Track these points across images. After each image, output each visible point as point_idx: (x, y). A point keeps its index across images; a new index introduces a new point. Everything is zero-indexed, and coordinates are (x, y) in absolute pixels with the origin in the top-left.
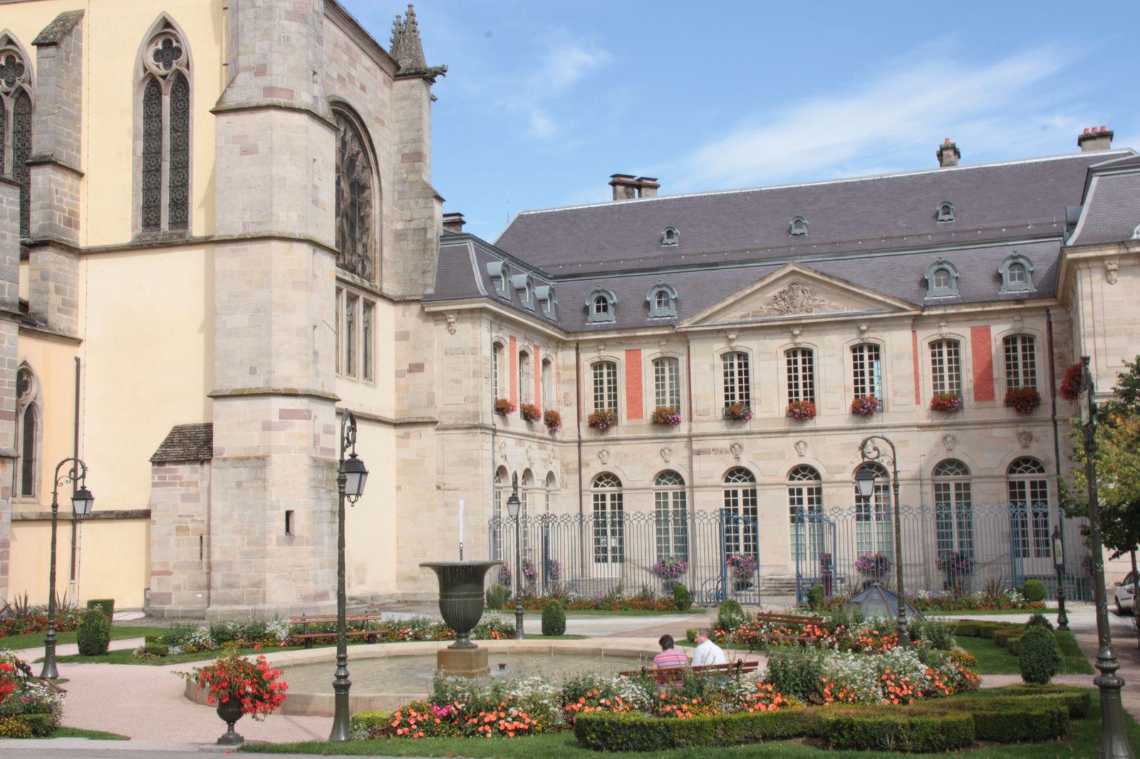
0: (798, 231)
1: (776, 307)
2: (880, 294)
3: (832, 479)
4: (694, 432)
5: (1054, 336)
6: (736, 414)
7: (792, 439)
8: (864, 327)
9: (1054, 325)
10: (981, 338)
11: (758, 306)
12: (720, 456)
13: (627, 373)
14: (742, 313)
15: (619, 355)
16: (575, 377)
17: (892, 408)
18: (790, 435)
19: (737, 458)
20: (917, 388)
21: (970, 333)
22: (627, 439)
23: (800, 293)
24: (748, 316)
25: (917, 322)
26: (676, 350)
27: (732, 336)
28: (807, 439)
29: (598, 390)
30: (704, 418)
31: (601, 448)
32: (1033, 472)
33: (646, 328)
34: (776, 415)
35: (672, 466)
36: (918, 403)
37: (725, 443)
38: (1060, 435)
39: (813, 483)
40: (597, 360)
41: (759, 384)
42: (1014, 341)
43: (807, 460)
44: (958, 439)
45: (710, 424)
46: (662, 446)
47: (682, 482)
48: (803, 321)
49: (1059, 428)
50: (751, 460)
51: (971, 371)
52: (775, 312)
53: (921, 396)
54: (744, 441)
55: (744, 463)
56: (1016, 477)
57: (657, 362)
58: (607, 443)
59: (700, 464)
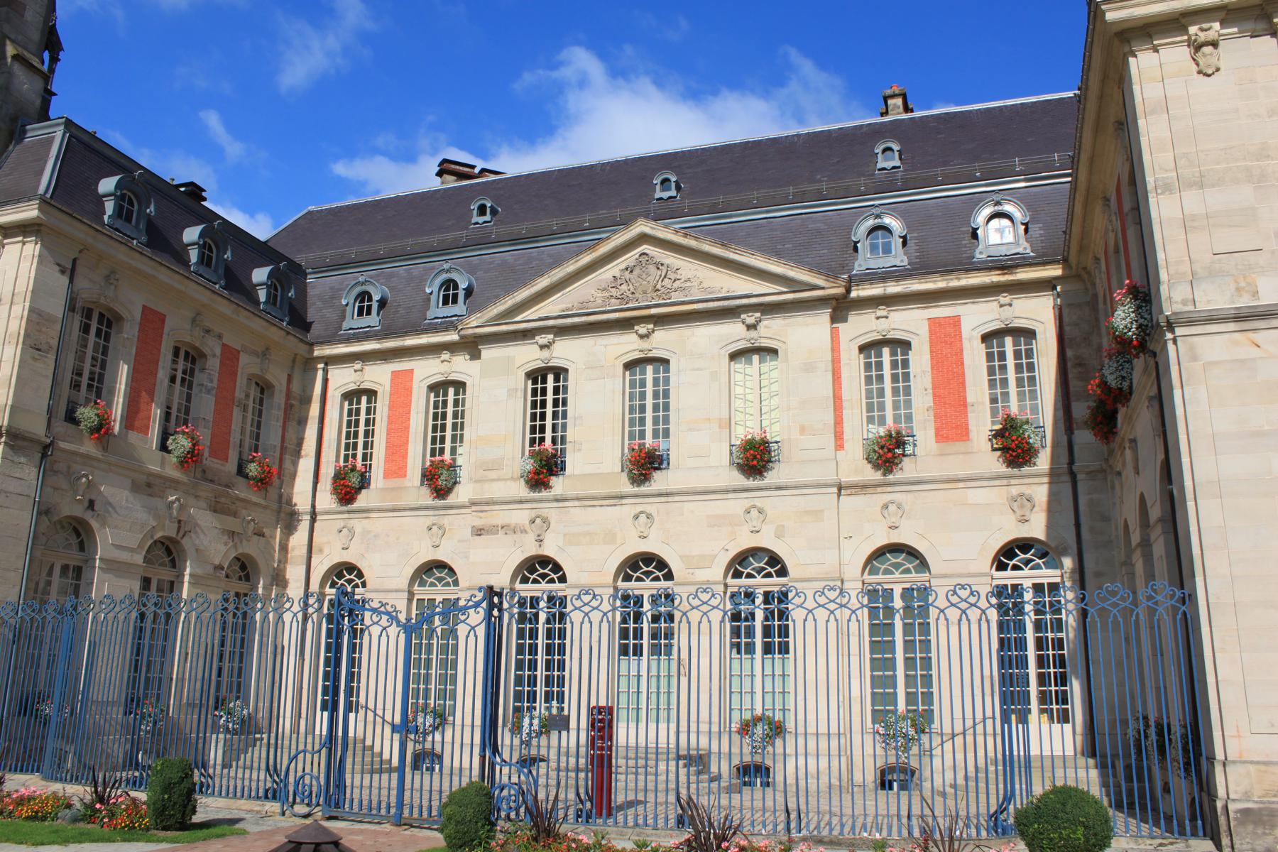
5: (1067, 328)
6: (546, 469)
7: (627, 510)
11: (587, 294)
12: (511, 537)
13: (391, 407)
14: (564, 306)
18: (624, 501)
20: (839, 422)
21: (927, 328)
22: (380, 511)
23: (652, 269)
24: (568, 309)
25: (841, 308)
26: (460, 366)
30: (493, 475)
37: (520, 516)
44: (907, 508)
45: (501, 484)
46: (429, 521)
48: (654, 311)
49: (1081, 487)
50: (561, 544)
51: (930, 391)
52: (613, 301)
55: (549, 550)
58: (352, 516)
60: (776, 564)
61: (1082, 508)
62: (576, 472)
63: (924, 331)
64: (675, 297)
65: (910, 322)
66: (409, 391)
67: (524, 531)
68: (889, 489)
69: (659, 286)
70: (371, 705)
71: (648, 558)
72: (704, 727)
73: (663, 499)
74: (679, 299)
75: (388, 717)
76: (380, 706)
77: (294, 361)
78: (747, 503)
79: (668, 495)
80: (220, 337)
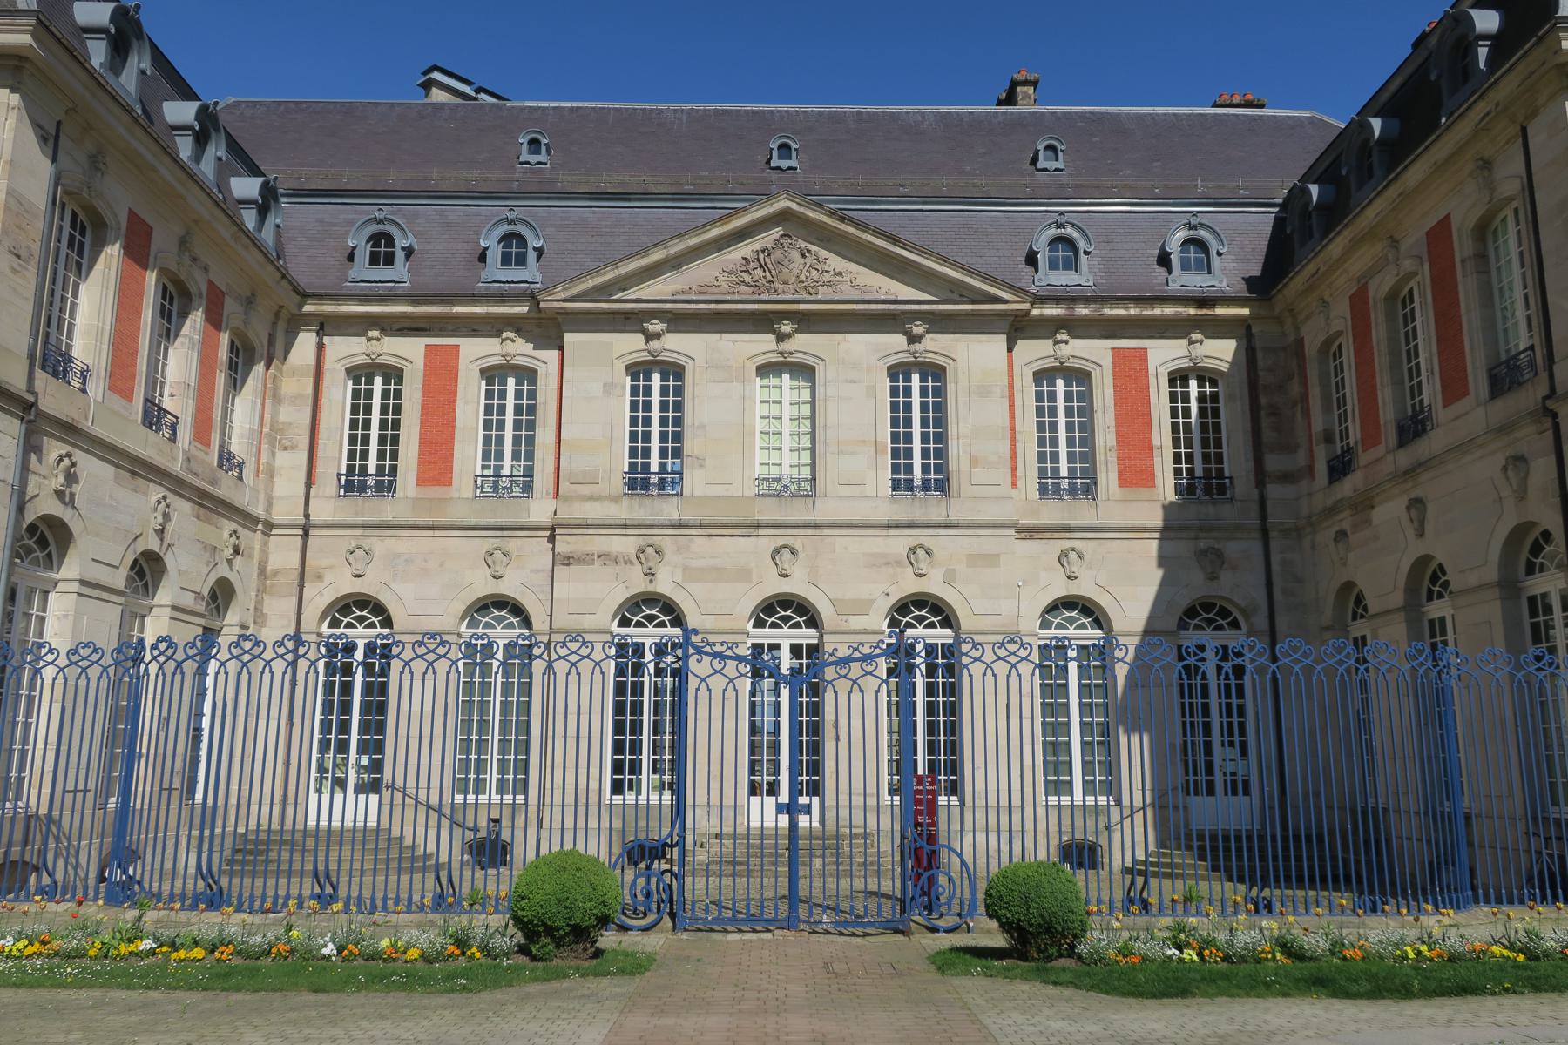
0: (785, 164)
1: (748, 279)
2: (955, 265)
3: (844, 626)
4: (561, 517)
7: (765, 543)
8: (918, 329)
9: (1260, 355)
10: (1131, 371)
12: (611, 569)
13: (426, 392)
14: (678, 287)
15: (410, 351)
16: (310, 390)
17: (966, 489)
18: (761, 532)
19: (650, 575)
23: (796, 255)
25: (1018, 328)
27: (655, 326)
28: (797, 543)
29: (359, 425)
31: (353, 543)
32: (1219, 628)
33: (475, 298)
34: (735, 491)
35: (507, 588)
36: (1014, 485)
37: (624, 544)
38: (1275, 560)
39: (807, 636)
40: (363, 360)
41: (703, 427)
42: (1185, 385)
43: (795, 586)
44: (1087, 557)
46: (489, 544)
47: (527, 622)
48: (802, 307)
49: (1274, 545)
52: (743, 288)
53: (1020, 472)
54: (666, 540)
55: (664, 585)
56: (1191, 639)
57: (489, 374)
59: (570, 585)
60: (941, 612)
61: (1275, 567)
62: (696, 493)
63: (1107, 361)
64: (824, 292)
65: (1095, 352)
66: (454, 375)
67: (628, 562)
68: (1067, 535)
69: (803, 277)
70: (399, 782)
71: (786, 601)
72: (858, 800)
73: (810, 532)
74: (825, 298)
75: (422, 796)
76: (411, 783)
77: (277, 315)
78: (913, 542)
79: (816, 527)
80: (206, 269)
